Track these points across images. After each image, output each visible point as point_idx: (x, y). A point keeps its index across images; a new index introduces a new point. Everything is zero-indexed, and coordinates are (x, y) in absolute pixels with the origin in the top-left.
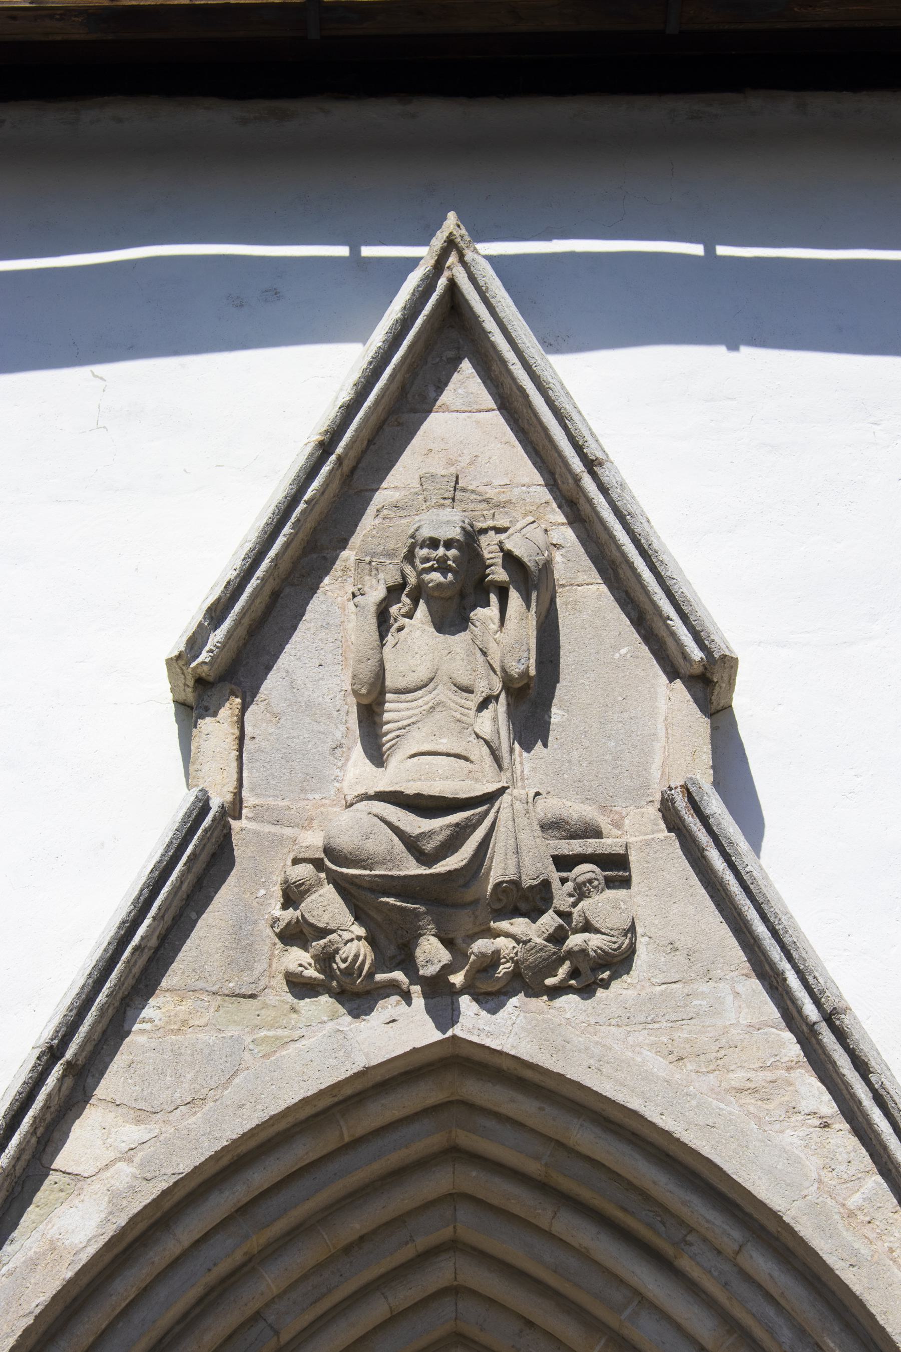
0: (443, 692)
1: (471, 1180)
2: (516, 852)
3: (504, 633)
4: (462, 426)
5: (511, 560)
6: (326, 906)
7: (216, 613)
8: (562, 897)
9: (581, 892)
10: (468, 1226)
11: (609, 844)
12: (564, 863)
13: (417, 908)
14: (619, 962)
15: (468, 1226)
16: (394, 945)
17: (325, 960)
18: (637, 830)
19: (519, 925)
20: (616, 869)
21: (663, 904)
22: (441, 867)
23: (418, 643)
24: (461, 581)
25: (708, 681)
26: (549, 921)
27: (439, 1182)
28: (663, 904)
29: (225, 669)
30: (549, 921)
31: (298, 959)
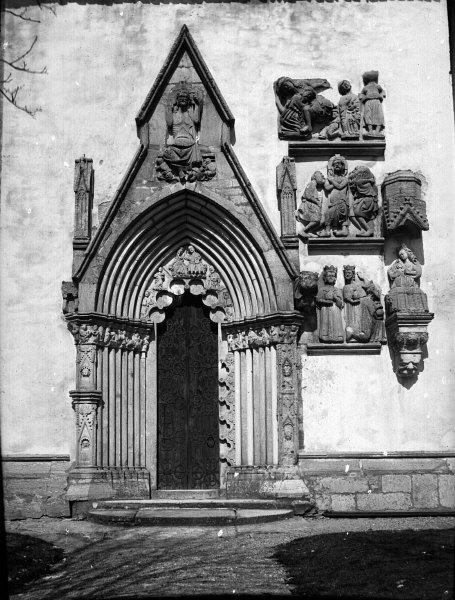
0: (184, 125)
1: (189, 212)
2: (195, 157)
3: (193, 112)
4: (185, 72)
5: (195, 99)
6: (164, 166)
7: (143, 109)
8: (204, 164)
9: (207, 163)
10: (190, 219)
11: (212, 154)
12: (206, 157)
13: (179, 164)
14: (213, 175)
15: (190, 219)
16: (176, 171)
17: (164, 175)
18: (214, 150)
19: (196, 169)
20: (213, 158)
21: (221, 166)
22: (185, 158)
23: (178, 116)
24: (185, 102)
25: (230, 123)
26: (202, 168)
27: (183, 212)
28: (221, 166)
29: (142, 121)
30: (202, 168)
31: (160, 174)
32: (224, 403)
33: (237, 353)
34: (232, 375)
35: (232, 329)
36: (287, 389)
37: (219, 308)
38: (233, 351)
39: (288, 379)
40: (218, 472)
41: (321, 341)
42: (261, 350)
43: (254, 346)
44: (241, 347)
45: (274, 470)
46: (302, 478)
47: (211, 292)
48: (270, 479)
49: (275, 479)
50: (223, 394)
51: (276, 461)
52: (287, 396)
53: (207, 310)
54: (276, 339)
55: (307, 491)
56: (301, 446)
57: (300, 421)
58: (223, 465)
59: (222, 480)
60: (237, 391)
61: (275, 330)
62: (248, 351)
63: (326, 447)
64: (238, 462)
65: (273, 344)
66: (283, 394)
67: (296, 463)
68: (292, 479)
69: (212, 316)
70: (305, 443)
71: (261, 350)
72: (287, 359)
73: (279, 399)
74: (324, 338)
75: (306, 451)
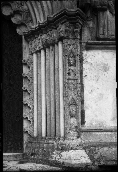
32: (26, 91)
33: (35, 55)
34: (32, 72)
35: (32, 35)
36: (72, 76)
37: (23, 24)
38: (32, 54)
39: (72, 68)
40: (22, 140)
41: (98, 39)
42: (51, 48)
43: (46, 46)
44: (38, 49)
45: (61, 141)
46: (84, 148)
47: (17, 12)
48: (58, 149)
49: (63, 150)
50: (25, 85)
51: (62, 135)
52: (72, 81)
53: (16, 26)
54: (62, 34)
55: (89, 161)
56: (83, 123)
57: (82, 102)
58: (26, 137)
59: (25, 146)
60: (35, 82)
61: (62, 28)
62: (42, 52)
63: (102, 123)
64: (35, 135)
65: (61, 39)
66: (69, 79)
67: (79, 136)
68: (76, 149)
69: (18, 30)
70: (86, 119)
71: (51, 48)
72: (72, 52)
73: (64, 83)
74: (101, 36)
75: (87, 126)
